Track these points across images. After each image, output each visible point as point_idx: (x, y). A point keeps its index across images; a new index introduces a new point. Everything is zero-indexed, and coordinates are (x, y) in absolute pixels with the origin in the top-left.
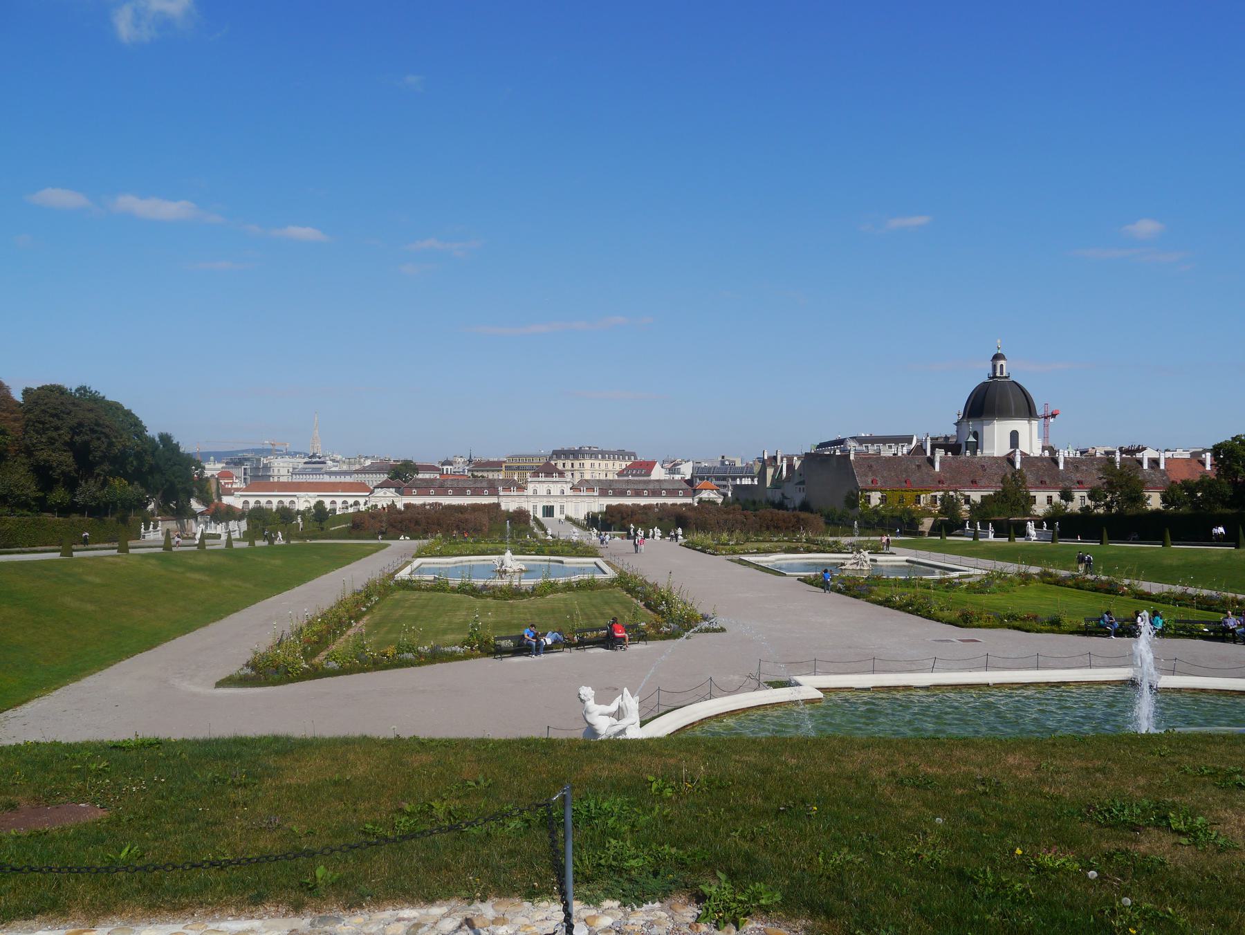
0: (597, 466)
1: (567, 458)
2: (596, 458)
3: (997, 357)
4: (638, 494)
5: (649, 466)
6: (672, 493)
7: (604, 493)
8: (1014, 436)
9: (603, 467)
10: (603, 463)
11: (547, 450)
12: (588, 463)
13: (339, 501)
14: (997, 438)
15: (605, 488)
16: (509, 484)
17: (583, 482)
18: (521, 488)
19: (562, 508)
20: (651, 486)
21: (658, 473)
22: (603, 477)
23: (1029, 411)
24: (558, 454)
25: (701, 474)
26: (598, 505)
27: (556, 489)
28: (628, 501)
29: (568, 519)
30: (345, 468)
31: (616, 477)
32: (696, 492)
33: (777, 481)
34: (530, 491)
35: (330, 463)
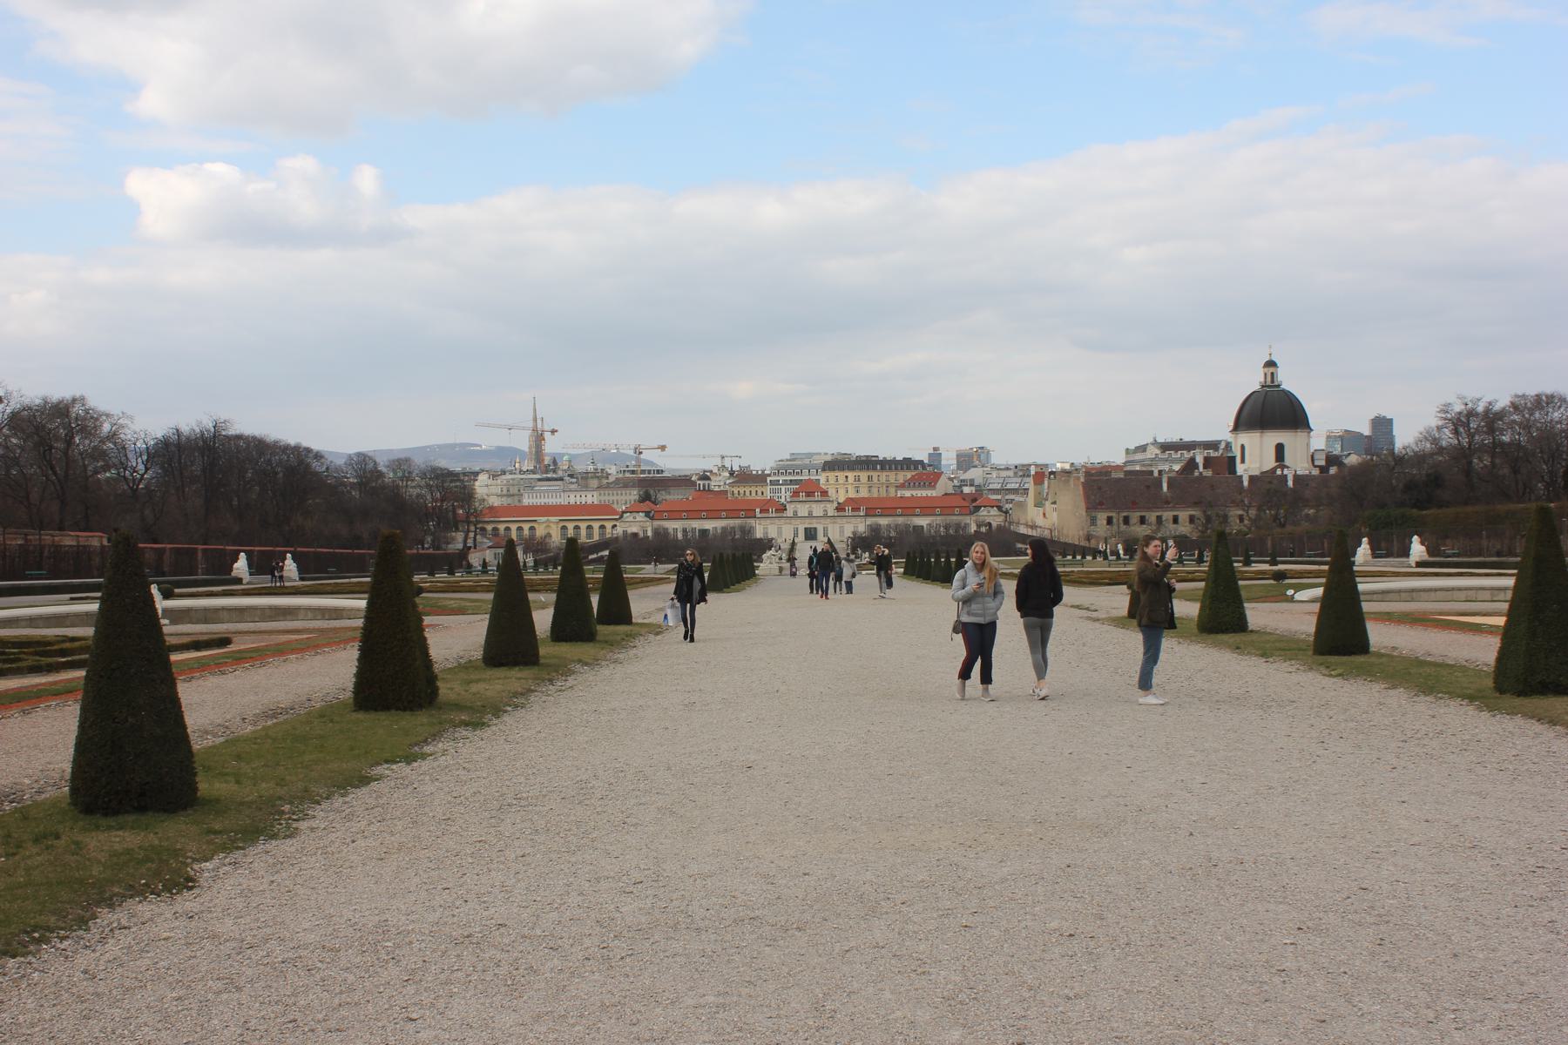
0: (875, 479)
2: (875, 469)
8: (1280, 449)
9: (883, 479)
12: (864, 475)
17: (849, 501)
18: (782, 508)
19: (825, 530)
26: (861, 526)
27: (818, 510)
34: (789, 513)
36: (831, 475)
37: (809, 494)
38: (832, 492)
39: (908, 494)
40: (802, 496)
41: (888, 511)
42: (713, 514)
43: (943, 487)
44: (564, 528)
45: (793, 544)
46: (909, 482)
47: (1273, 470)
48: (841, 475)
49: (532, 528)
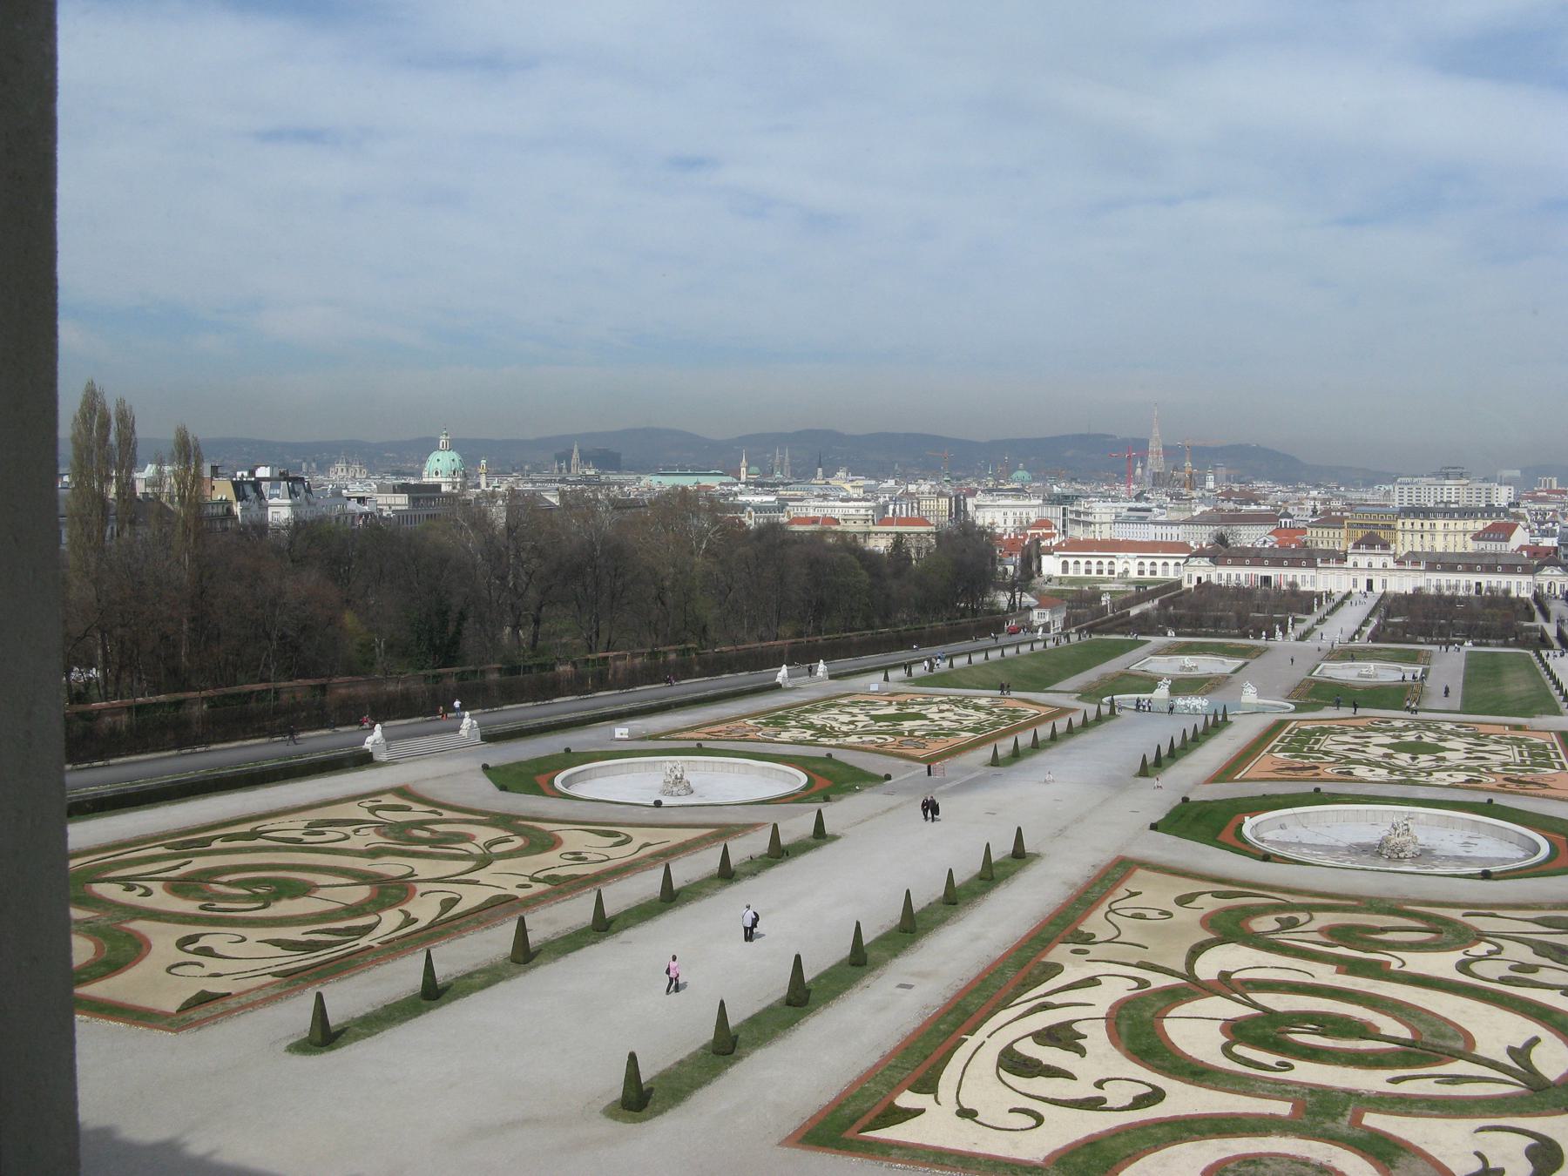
1: (1417, 517)
2: (1452, 517)
4: (1470, 569)
5: (1504, 532)
7: (1431, 568)
10: (1460, 525)
12: (1440, 524)
17: (1412, 554)
18: (1342, 558)
19: (1384, 582)
20: (1486, 561)
21: (1520, 538)
27: (1378, 562)
30: (1174, 516)
34: (1349, 564)
35: (1156, 510)
36: (1408, 522)
37: (1371, 546)
40: (1363, 549)
41: (1451, 568)
42: (1277, 563)
43: (1520, 538)
44: (1141, 564)
45: (1349, 595)
48: (1418, 523)
49: (1111, 563)
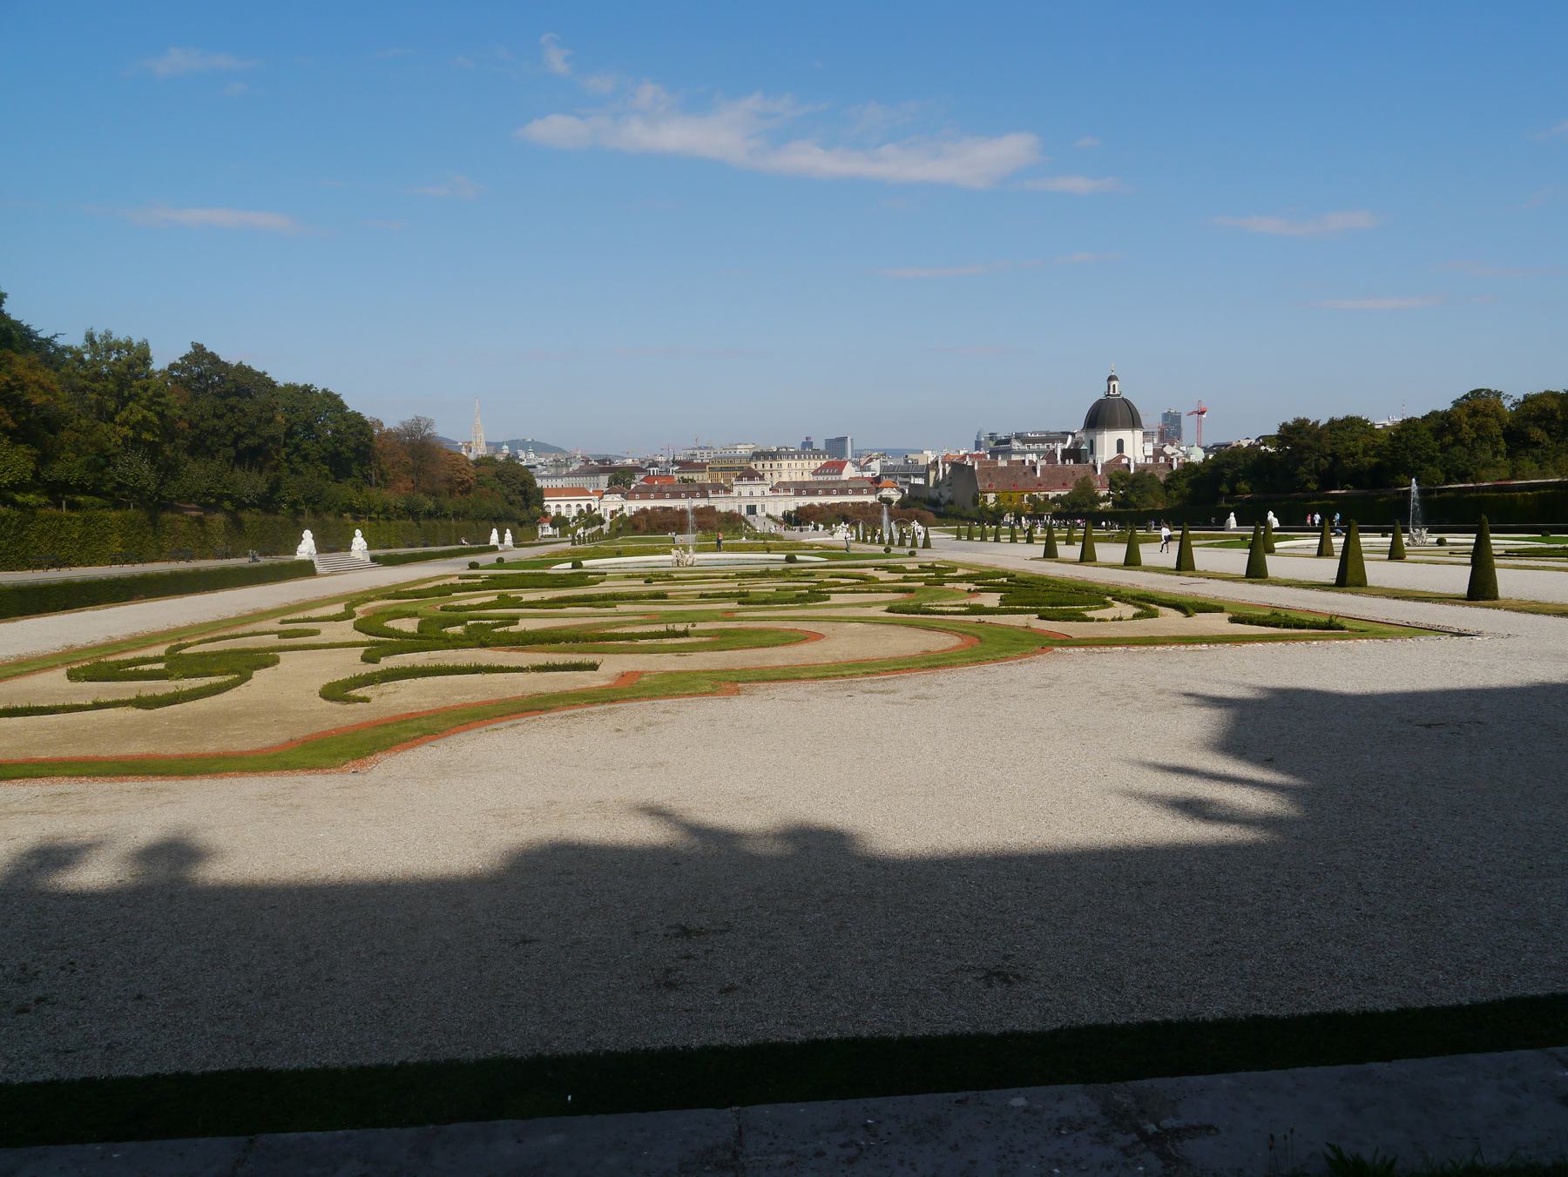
3: (1111, 378)
4: (828, 493)
6: (858, 491)
7: (798, 493)
8: (1120, 443)
10: (799, 463)
11: (744, 450)
12: (785, 463)
13: (563, 504)
14: (1106, 445)
15: (801, 489)
16: (717, 488)
18: (728, 491)
21: (849, 472)
22: (799, 479)
23: (1133, 421)
24: (757, 456)
25: (888, 472)
26: (792, 503)
27: (757, 491)
28: (816, 501)
29: (768, 516)
31: (812, 478)
32: (878, 490)
33: (936, 482)
34: (735, 494)
37: (751, 478)
38: (767, 476)
39: (821, 478)
46: (823, 467)
47: (1118, 459)
